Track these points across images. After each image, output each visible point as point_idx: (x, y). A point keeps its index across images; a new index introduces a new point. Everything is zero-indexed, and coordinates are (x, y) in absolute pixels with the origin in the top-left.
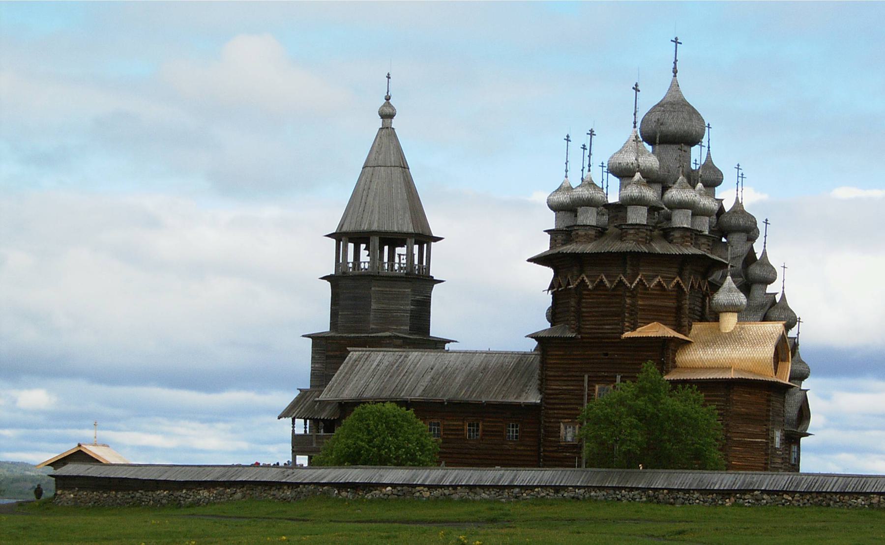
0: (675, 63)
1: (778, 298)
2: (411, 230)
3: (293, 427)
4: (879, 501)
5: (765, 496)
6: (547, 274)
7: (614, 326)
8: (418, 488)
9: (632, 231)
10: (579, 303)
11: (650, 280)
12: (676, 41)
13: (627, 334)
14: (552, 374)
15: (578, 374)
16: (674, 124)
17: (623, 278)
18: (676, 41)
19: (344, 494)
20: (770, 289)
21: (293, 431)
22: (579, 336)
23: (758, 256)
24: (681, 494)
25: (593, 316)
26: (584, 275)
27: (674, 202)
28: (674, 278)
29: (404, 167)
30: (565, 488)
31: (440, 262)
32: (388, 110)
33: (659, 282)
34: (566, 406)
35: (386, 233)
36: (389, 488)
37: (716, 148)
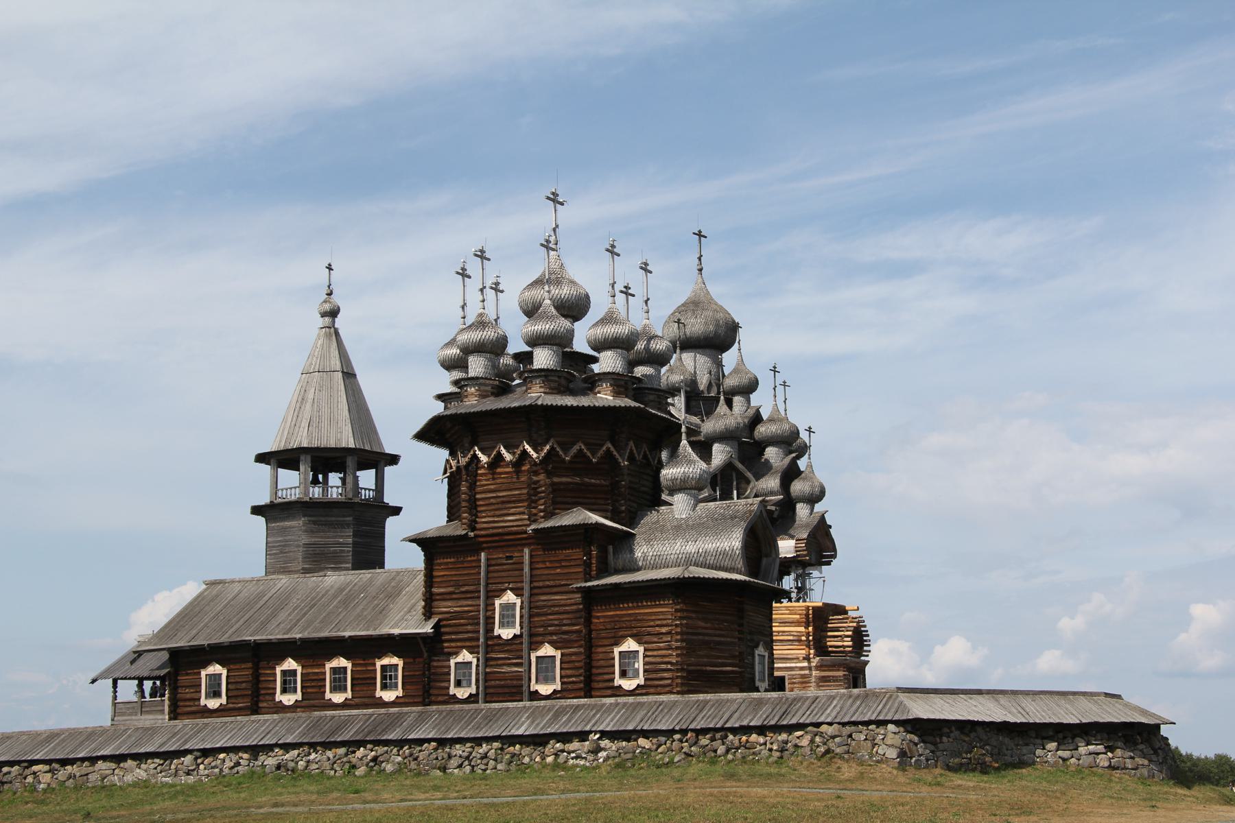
0: (700, 259)
2: (352, 445)
3: (115, 692)
4: (812, 741)
5: (605, 743)
6: (444, 454)
7: (518, 517)
8: (35, 768)
11: (566, 447)
12: (700, 234)
14: (442, 590)
15: (471, 588)
16: (696, 326)
17: (527, 447)
18: (700, 234)
20: (819, 507)
21: (115, 698)
22: (472, 534)
24: (458, 750)
28: (602, 445)
29: (349, 375)
30: (269, 748)
32: (327, 307)
33: (581, 450)
34: (460, 636)
35: (318, 449)
37: (751, 353)
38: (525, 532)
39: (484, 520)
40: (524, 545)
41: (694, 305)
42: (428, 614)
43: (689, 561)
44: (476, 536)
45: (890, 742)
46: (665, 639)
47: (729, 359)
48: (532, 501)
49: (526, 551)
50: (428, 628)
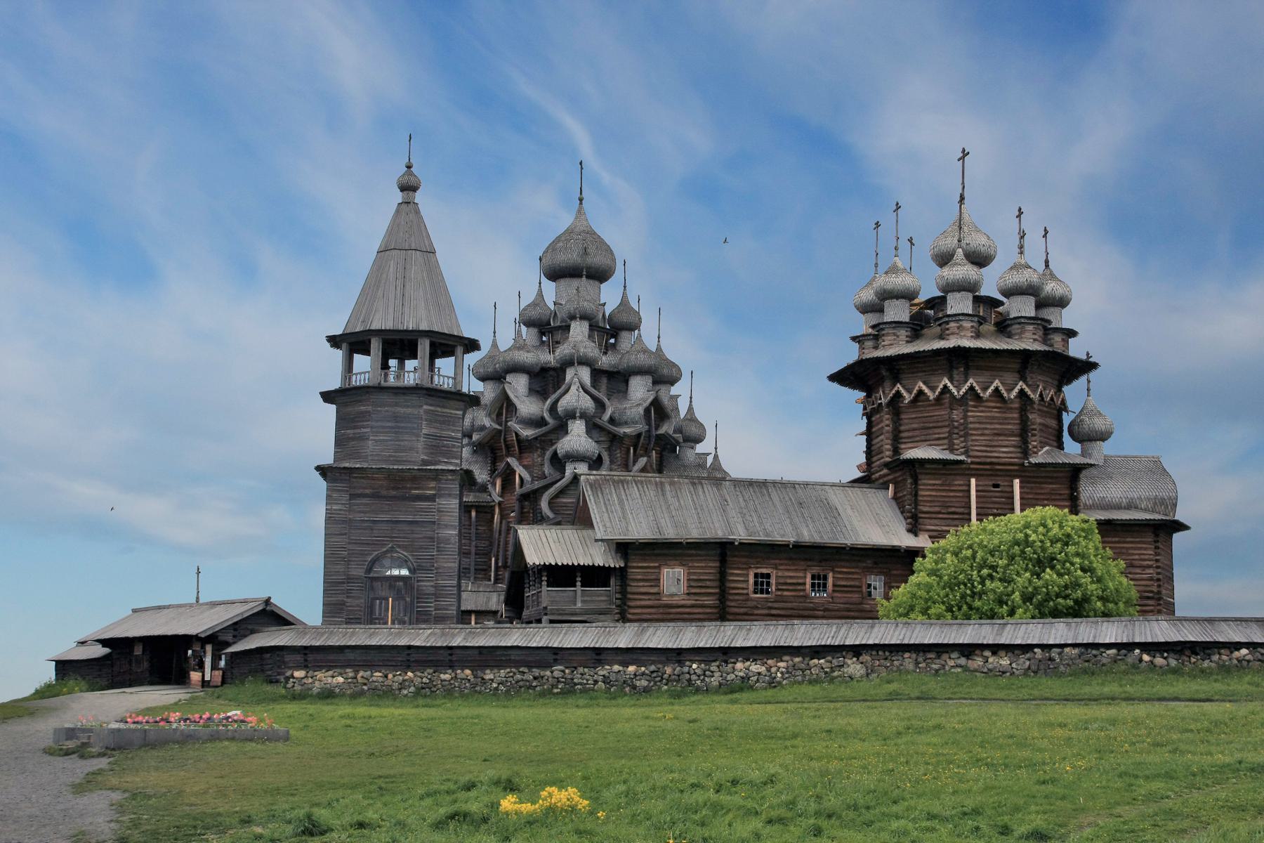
1: (710, 460)
9: (1031, 327)
10: (965, 417)
13: (1033, 460)
19: (1159, 661)
23: (683, 412)
25: (982, 435)
26: (971, 381)
27: (1054, 298)
36: (1244, 651)
38: (1023, 464)
40: (1017, 477)
43: (1131, 506)
44: (972, 463)
46: (1148, 571)
49: (1017, 482)
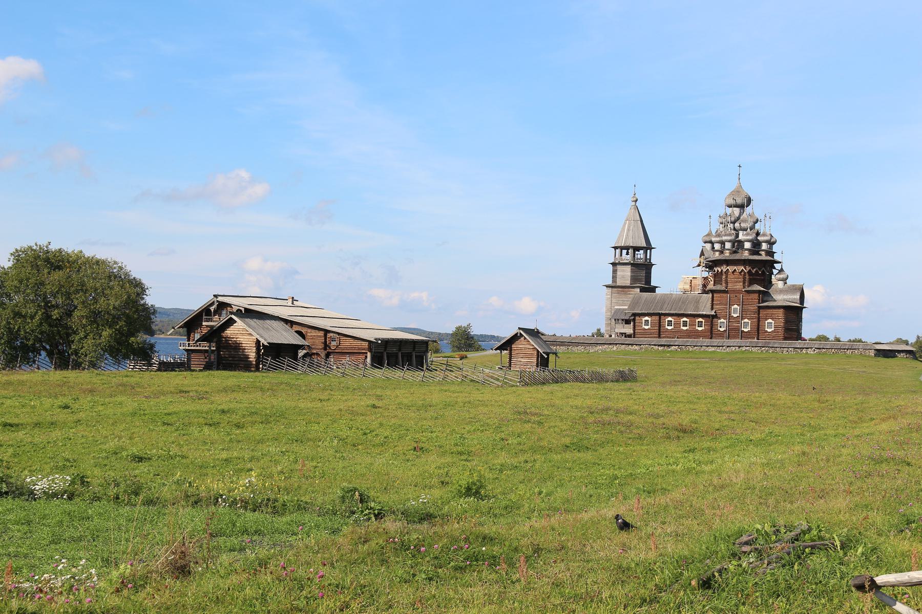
31: (655, 257)
39: (730, 286)
41: (738, 191)
42: (712, 309)
45: (872, 353)
47: (748, 210)
48: (744, 283)
50: (713, 313)
